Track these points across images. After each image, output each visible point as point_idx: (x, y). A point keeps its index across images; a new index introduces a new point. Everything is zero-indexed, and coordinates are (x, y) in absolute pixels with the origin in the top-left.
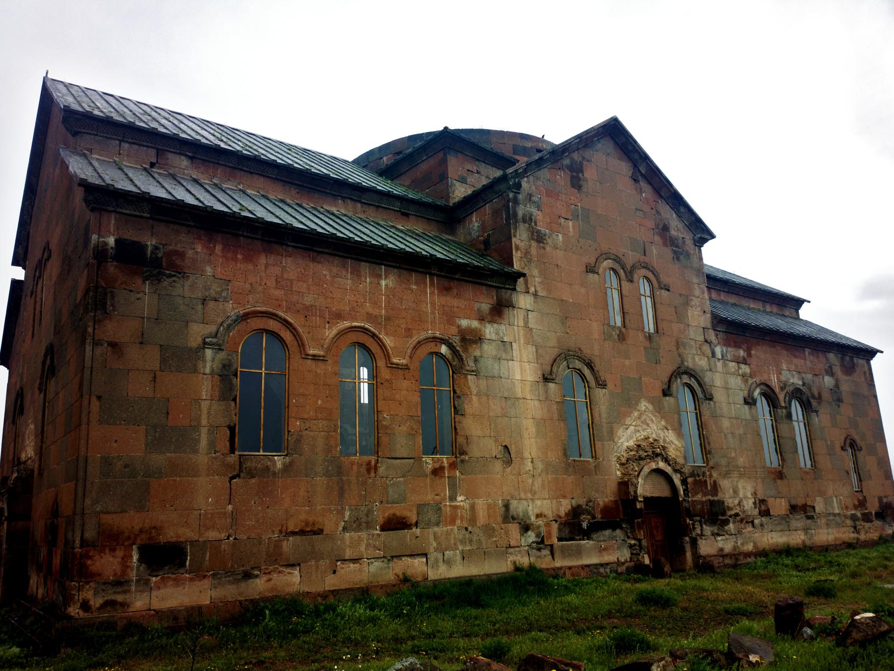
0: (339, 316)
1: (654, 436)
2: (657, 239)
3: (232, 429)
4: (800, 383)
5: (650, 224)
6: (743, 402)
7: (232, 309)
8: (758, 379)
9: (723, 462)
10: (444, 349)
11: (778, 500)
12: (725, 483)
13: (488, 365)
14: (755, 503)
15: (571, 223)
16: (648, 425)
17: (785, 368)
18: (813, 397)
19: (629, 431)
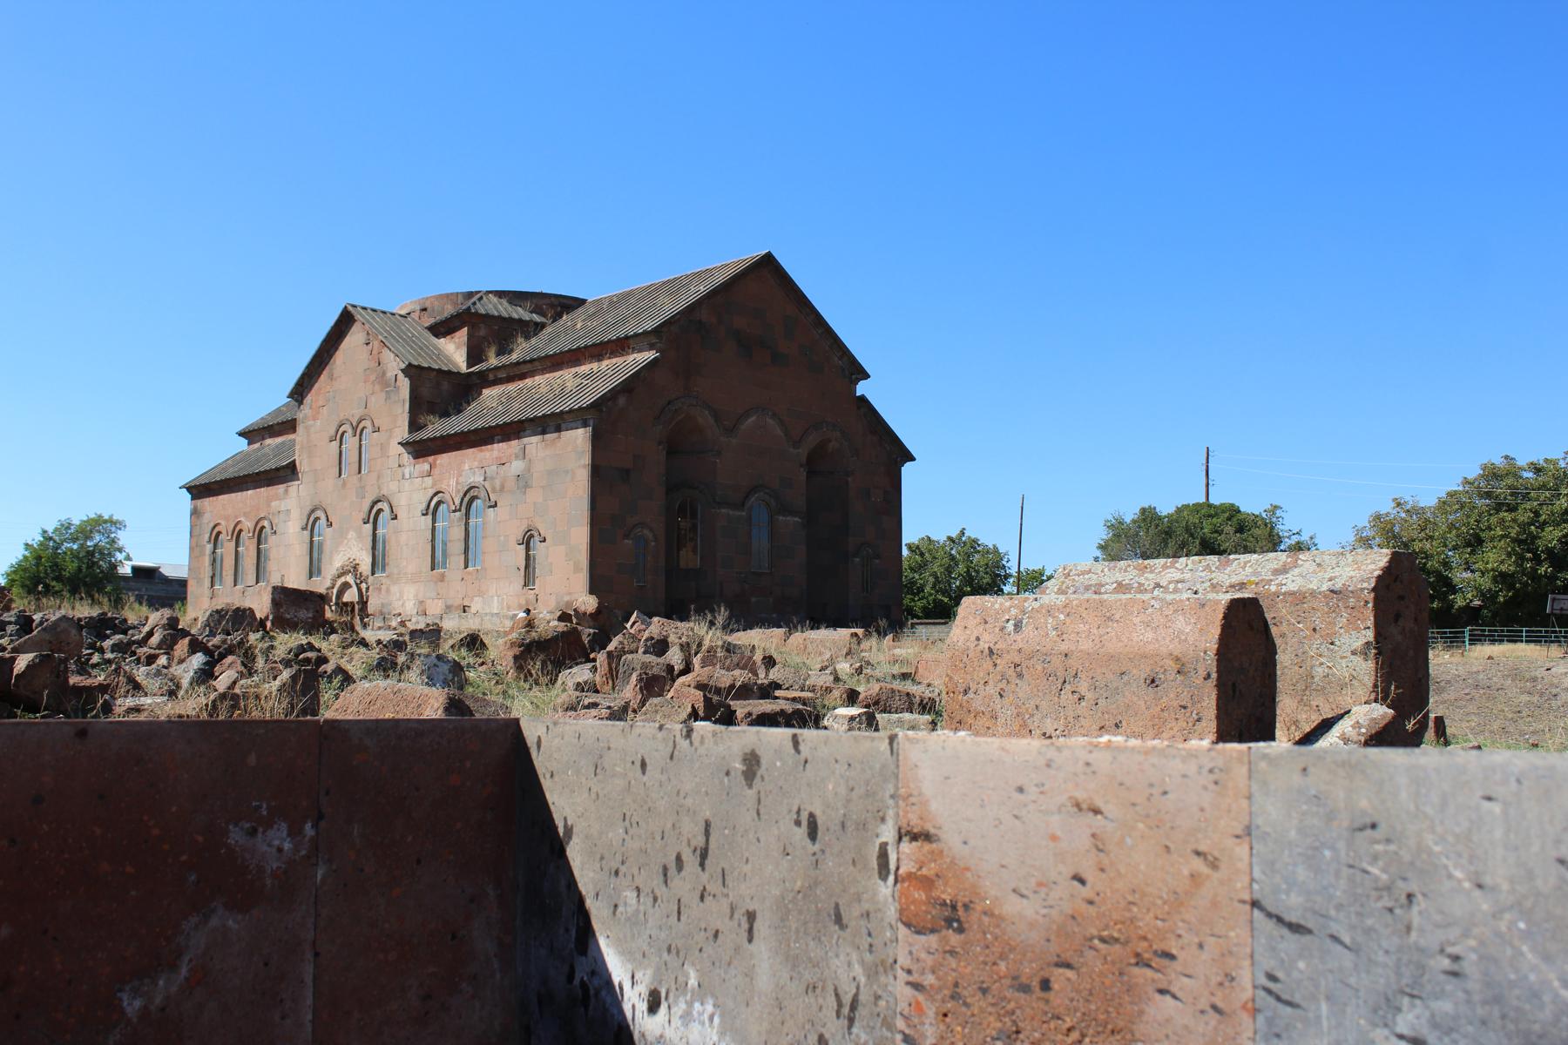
0: (236, 517)
1: (354, 557)
2: (377, 387)
3: (212, 578)
4: (482, 478)
5: (373, 377)
6: (420, 514)
7: (212, 525)
8: (434, 491)
9: (395, 571)
10: (266, 523)
11: (436, 601)
12: (394, 589)
13: (280, 529)
14: (415, 604)
15: (325, 408)
16: (351, 549)
17: (467, 467)
18: (494, 490)
19: (340, 555)
